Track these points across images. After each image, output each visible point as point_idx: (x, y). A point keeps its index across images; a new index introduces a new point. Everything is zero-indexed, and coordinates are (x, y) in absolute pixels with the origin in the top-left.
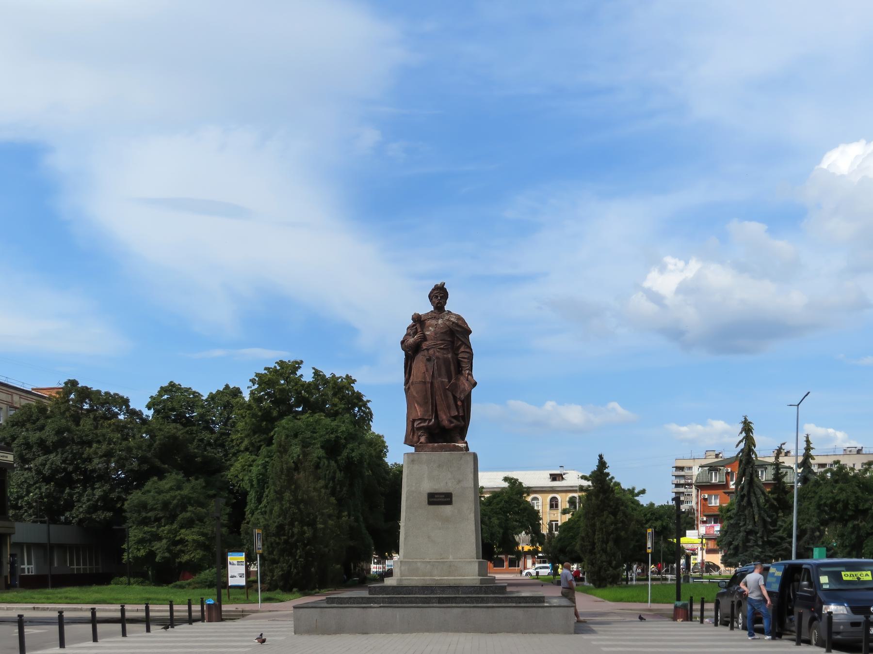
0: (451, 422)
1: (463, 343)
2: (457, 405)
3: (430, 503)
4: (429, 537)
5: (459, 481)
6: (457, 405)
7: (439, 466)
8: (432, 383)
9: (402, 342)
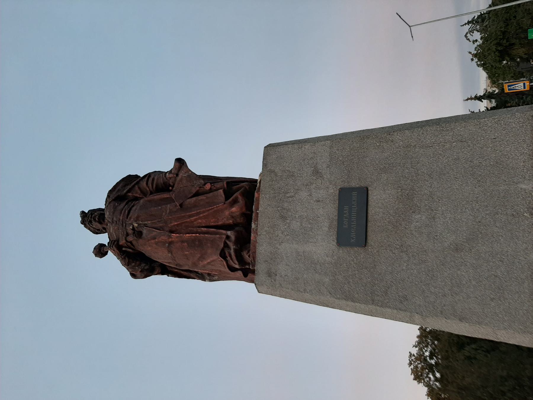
0: (235, 201)
1: (138, 183)
2: (211, 191)
3: (363, 241)
4: (457, 249)
5: (317, 172)
6: (211, 191)
7: (283, 218)
8: (172, 232)
9: (134, 276)
